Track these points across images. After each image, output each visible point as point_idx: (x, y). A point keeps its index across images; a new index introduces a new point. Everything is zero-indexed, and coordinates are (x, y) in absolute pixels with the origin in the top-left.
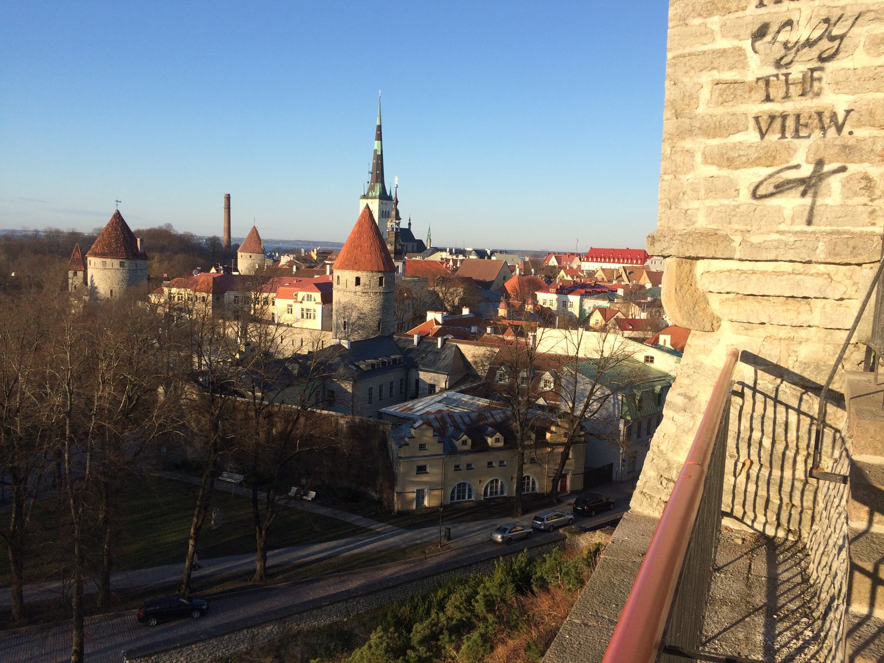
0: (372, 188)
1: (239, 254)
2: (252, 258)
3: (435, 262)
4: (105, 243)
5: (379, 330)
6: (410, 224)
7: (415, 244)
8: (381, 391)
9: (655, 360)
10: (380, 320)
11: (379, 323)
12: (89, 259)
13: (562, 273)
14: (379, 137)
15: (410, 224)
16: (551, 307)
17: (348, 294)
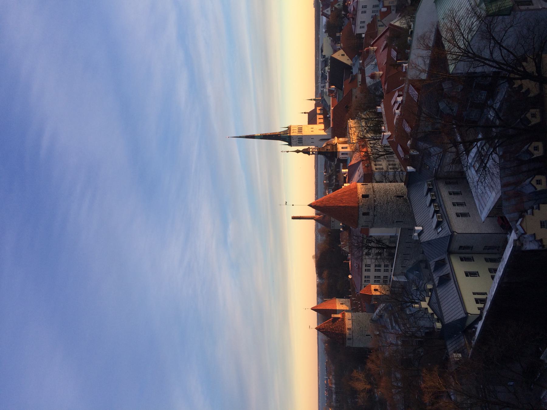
1: (332, 228)
2: (334, 221)
5: (403, 197)
6: (305, 113)
8: (459, 204)
13: (336, 6)
14: (253, 137)
15: (305, 113)
16: (367, 23)
17: (375, 220)
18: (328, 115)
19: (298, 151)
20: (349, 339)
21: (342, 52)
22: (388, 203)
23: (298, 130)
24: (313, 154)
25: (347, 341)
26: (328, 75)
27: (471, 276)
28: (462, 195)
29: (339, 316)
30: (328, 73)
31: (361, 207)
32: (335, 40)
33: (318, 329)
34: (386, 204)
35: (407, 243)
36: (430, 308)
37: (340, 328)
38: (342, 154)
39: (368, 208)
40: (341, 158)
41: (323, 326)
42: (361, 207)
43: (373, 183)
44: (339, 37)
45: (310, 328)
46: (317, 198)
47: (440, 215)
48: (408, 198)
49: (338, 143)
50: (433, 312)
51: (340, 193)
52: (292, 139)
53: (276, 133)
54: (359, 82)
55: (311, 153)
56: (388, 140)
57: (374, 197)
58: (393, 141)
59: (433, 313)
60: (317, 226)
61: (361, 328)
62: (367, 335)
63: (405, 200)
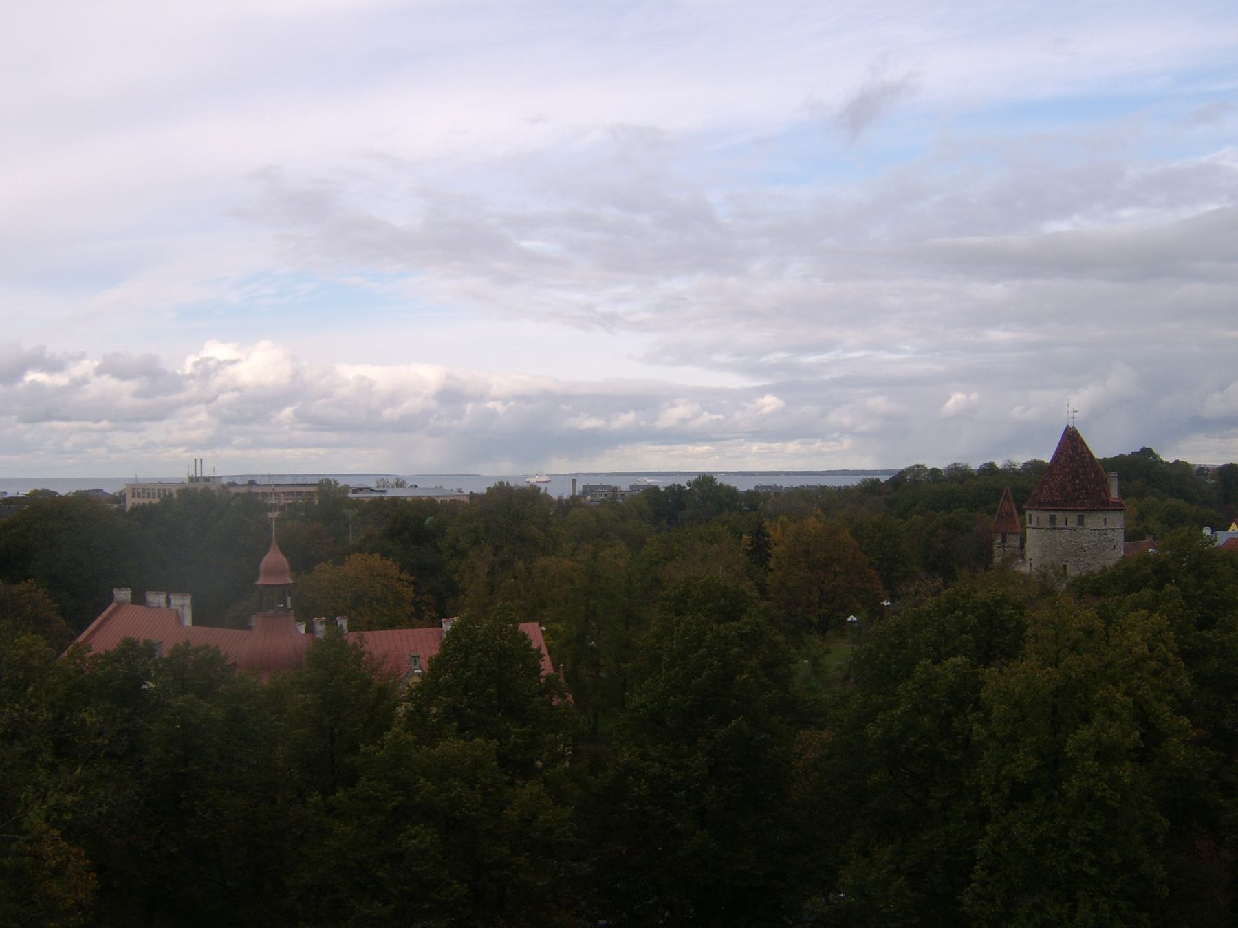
12: (1028, 513)
20: (1053, 519)
25: (1044, 516)
37: (1081, 496)
45: (1074, 412)
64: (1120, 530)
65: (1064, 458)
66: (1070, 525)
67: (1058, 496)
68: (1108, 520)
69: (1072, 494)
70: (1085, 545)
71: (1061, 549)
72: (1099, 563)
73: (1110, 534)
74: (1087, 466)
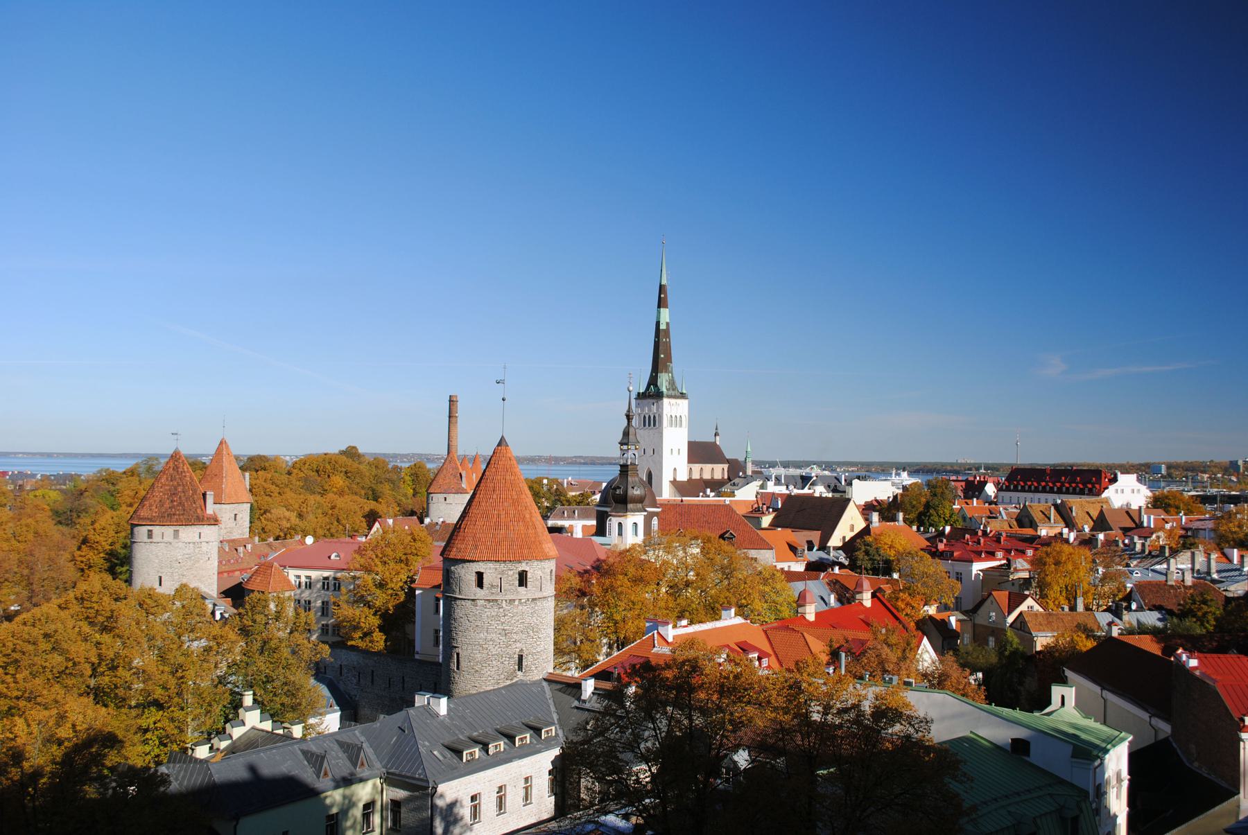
0: (653, 381)
2: (447, 501)
3: (728, 509)
4: (155, 501)
5: (520, 668)
7: (726, 466)
9: (1033, 749)
10: (522, 650)
11: (521, 658)
15: (716, 435)
18: (711, 491)
19: (629, 417)
21: (860, 525)
22: (505, 633)
23: (676, 416)
24: (624, 452)
26: (806, 491)
27: (327, 826)
28: (524, 806)
29: (211, 508)
30: (811, 491)
31: (496, 569)
32: (887, 510)
33: (175, 457)
34: (504, 629)
35: (402, 681)
36: (246, 731)
37: (177, 512)
38: (620, 524)
39: (492, 586)
40: (610, 520)
41: (183, 469)
42: (496, 569)
43: (553, 598)
44: (894, 519)
46: (521, 460)
47: (477, 757)
48: (517, 682)
49: (646, 513)
50: (234, 738)
51: (531, 517)
52: (654, 401)
53: (671, 363)
54: (789, 567)
55: (625, 447)
56: (656, 635)
57: (521, 600)
58: (654, 646)
59: (231, 737)
60: (430, 459)
61: (179, 565)
62: (160, 578)
63: (513, 675)
64: (214, 543)
65: (165, 476)
66: (166, 539)
67: (156, 512)
68: (202, 535)
69: (169, 510)
70: (180, 557)
71: (157, 561)
72: (192, 574)
73: (205, 547)
74: (187, 483)
